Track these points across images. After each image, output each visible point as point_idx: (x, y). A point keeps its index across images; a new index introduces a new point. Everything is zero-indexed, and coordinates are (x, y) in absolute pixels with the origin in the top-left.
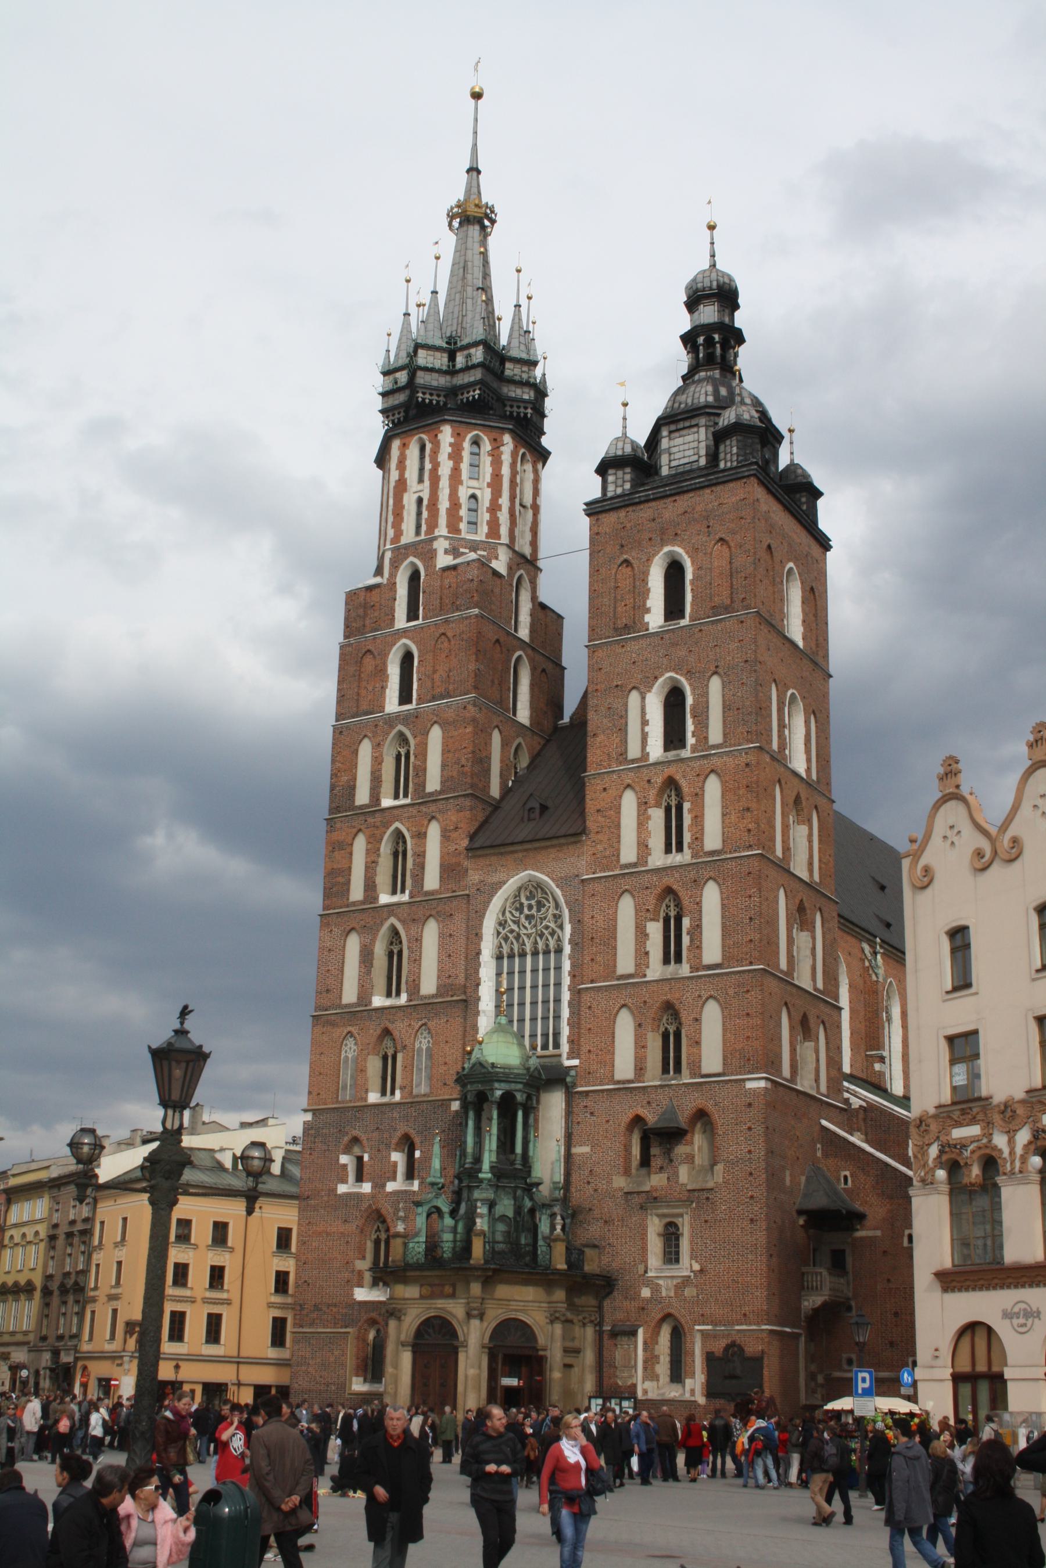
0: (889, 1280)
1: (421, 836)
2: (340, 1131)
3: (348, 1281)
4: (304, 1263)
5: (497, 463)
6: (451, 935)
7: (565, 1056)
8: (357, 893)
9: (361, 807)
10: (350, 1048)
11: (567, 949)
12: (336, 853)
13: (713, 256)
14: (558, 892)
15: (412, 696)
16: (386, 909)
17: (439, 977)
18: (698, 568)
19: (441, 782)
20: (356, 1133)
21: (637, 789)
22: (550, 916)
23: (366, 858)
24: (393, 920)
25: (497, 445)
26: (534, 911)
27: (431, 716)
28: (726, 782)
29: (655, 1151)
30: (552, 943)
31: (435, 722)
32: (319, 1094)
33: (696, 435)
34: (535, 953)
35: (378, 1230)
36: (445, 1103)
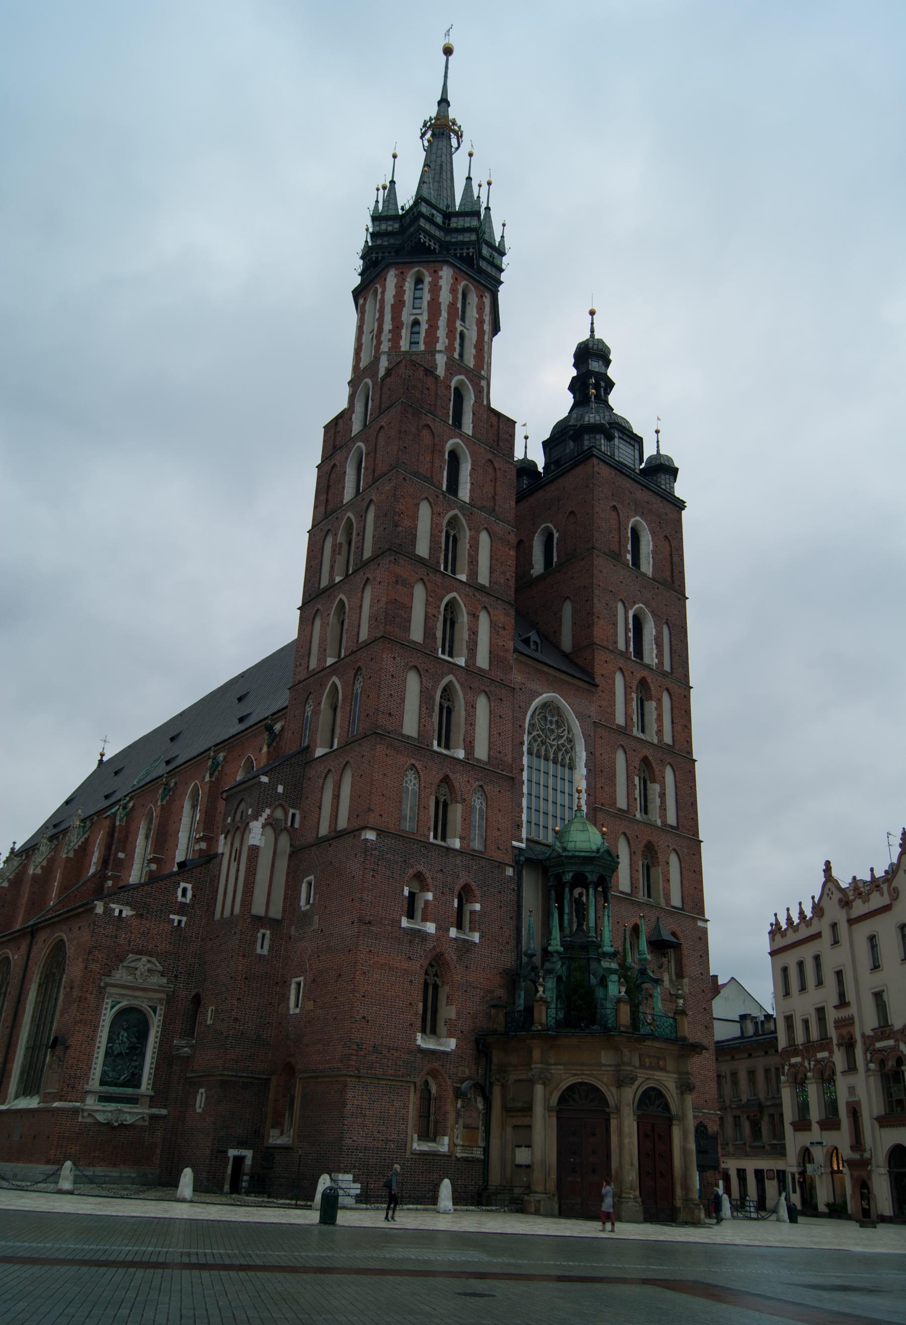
1: (474, 616)
2: (405, 861)
3: (411, 1025)
4: (364, 996)
6: (500, 716)
9: (421, 558)
10: (411, 781)
11: (581, 771)
12: (399, 587)
13: (592, 331)
16: (446, 664)
17: (490, 749)
18: (655, 546)
19: (490, 582)
20: (421, 868)
21: (626, 673)
22: (565, 737)
23: (426, 607)
24: (450, 677)
26: (553, 727)
27: (483, 522)
30: (568, 761)
31: (486, 529)
32: (381, 815)
33: (632, 452)
35: (426, 973)
36: (501, 865)
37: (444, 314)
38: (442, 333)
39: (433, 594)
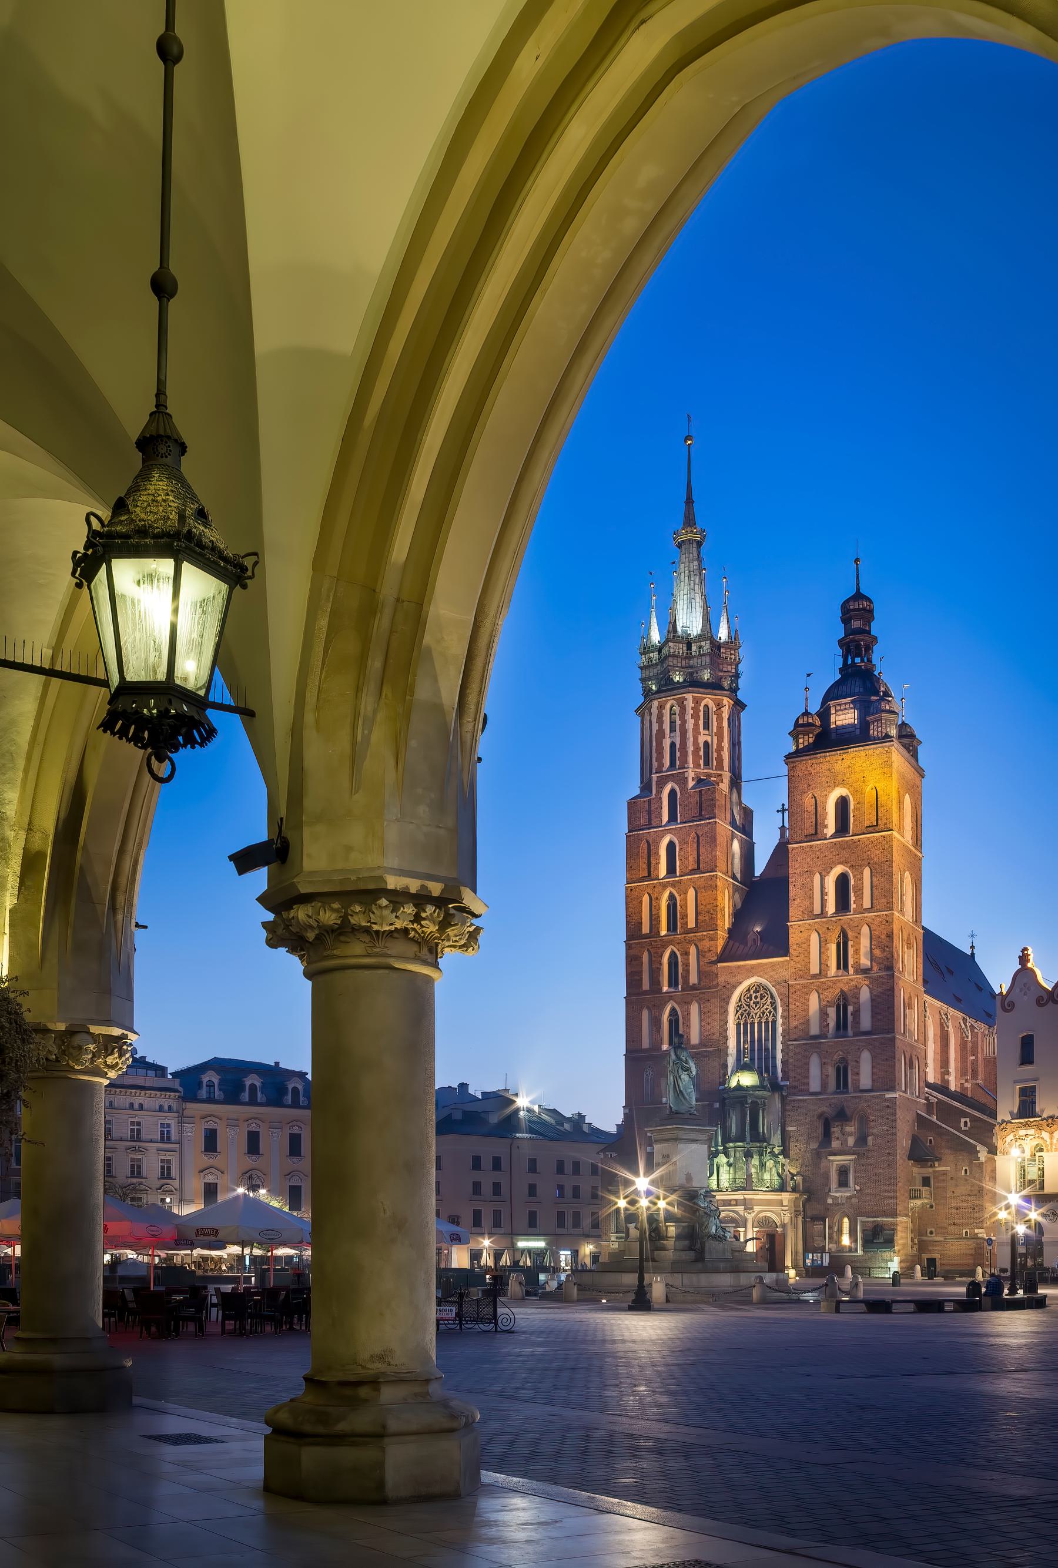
0: (953, 1192)
1: (687, 954)
5: (720, 719)
6: (709, 1012)
7: (780, 1079)
8: (646, 985)
9: (646, 937)
12: (633, 962)
14: (773, 990)
15: (676, 870)
21: (820, 933)
25: (719, 706)
28: (874, 930)
29: (835, 1130)
30: (770, 1019)
34: (760, 1023)
37: (654, 744)
38: (654, 759)
39: (655, 955)
